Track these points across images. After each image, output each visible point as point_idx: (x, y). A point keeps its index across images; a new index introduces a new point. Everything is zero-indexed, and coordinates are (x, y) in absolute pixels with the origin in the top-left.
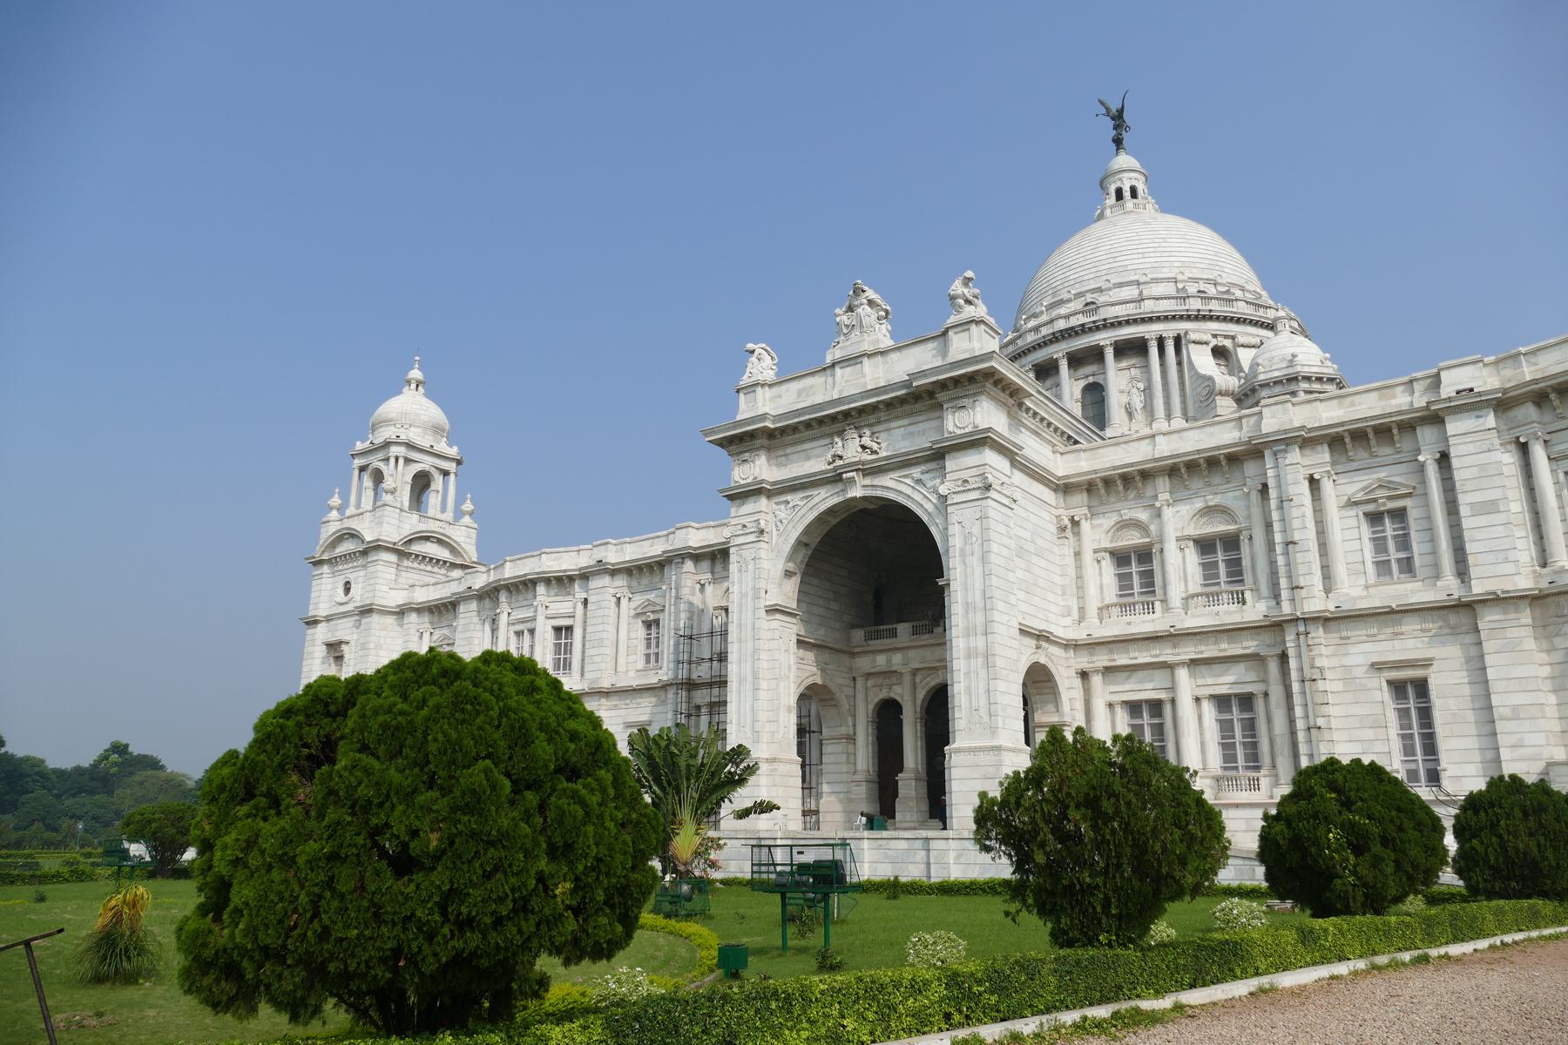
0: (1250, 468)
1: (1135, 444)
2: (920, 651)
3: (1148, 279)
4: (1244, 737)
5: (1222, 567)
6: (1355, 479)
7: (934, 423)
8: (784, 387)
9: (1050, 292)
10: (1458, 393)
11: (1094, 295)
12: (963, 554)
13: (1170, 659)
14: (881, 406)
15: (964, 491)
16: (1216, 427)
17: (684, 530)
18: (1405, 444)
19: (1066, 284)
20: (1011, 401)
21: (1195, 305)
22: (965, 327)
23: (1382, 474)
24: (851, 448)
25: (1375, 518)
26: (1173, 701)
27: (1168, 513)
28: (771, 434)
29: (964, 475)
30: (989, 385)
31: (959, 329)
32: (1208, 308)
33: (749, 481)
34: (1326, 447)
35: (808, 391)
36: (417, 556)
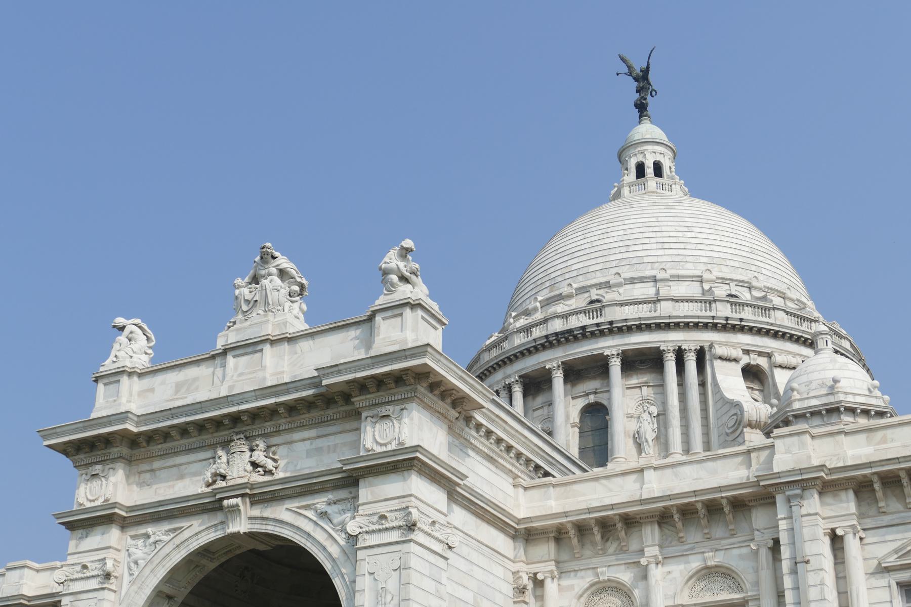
0: (759, 518)
1: (619, 480)
3: (667, 276)
6: (888, 538)
7: (349, 437)
8: (160, 378)
9: (548, 284)
11: (601, 292)
14: (281, 410)
15: (380, 530)
16: (720, 463)
17: (18, 572)
19: (567, 276)
20: (454, 413)
21: (723, 311)
22: (397, 311)
29: (382, 508)
30: (422, 389)
31: (389, 313)
32: (738, 316)
34: (851, 494)
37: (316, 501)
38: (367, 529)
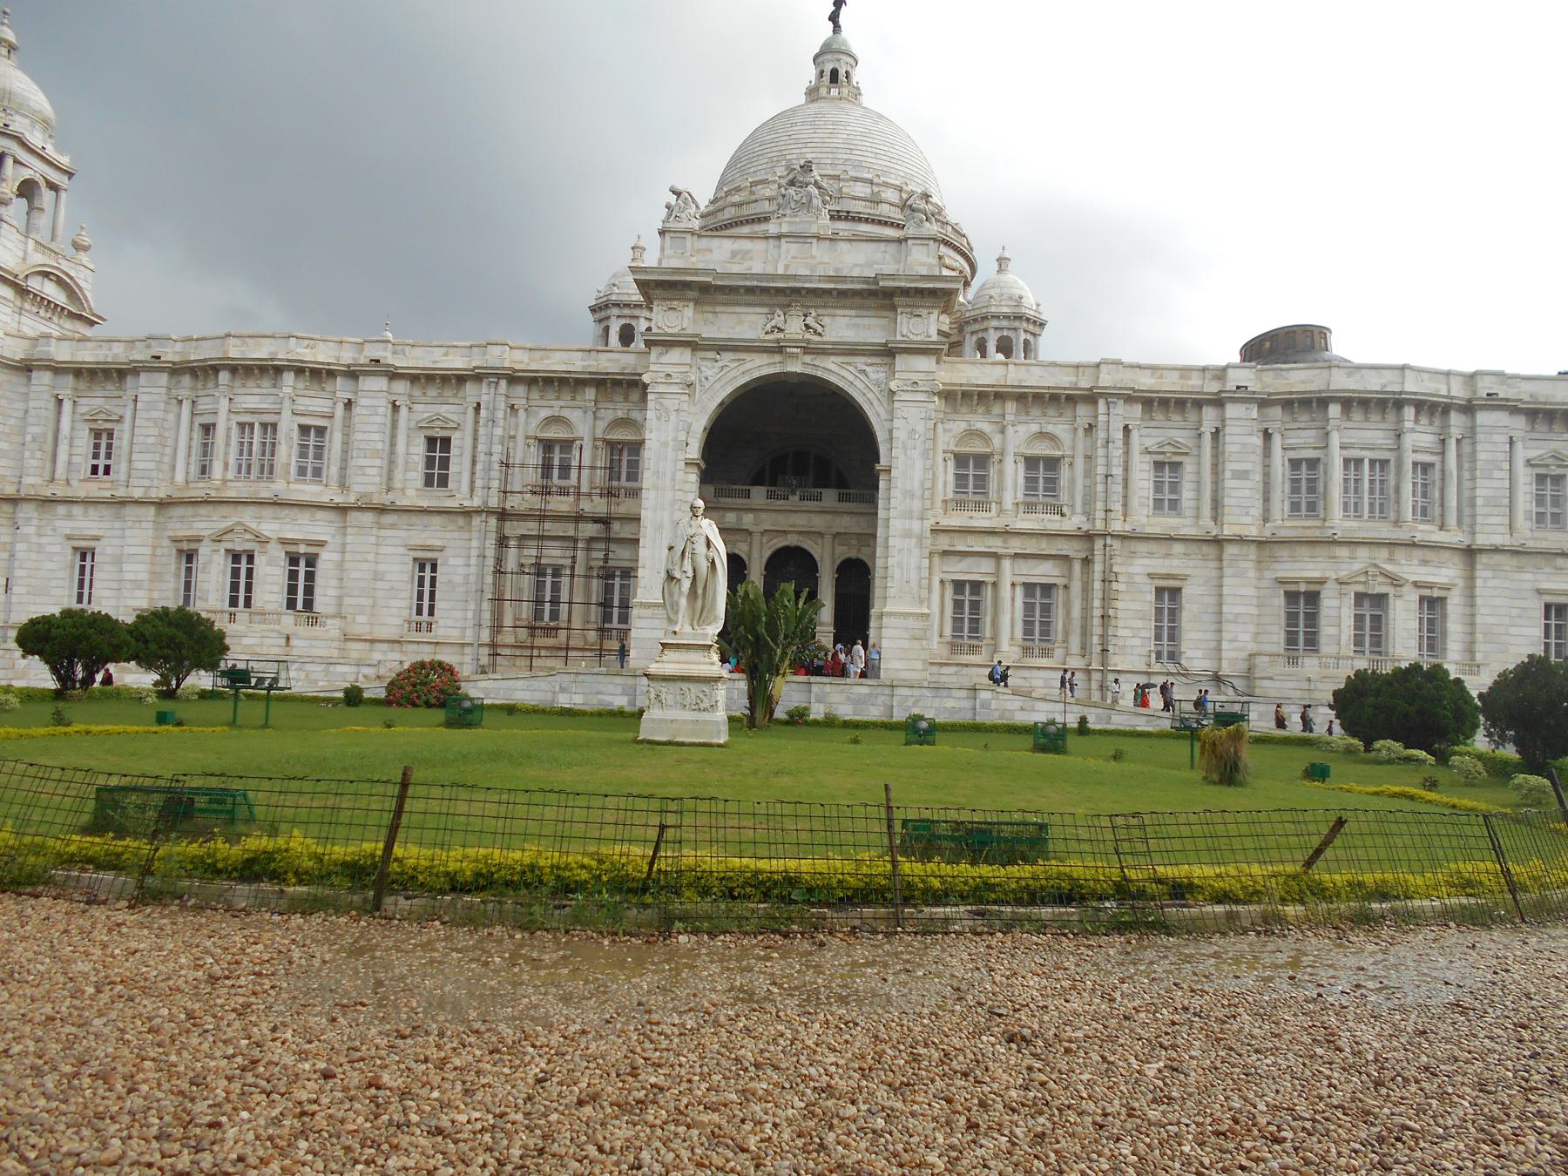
0: (1083, 410)
2: (774, 515)
5: (1041, 480)
9: (784, 163)
10: (1238, 388)
13: (1000, 551)
16: (1057, 369)
18: (1192, 416)
24: (794, 327)
25: (1159, 466)
26: (995, 584)
27: (1010, 430)
28: (705, 289)
29: (915, 377)
31: (919, 242)
33: (675, 331)
35: (745, 255)
36: (35, 295)
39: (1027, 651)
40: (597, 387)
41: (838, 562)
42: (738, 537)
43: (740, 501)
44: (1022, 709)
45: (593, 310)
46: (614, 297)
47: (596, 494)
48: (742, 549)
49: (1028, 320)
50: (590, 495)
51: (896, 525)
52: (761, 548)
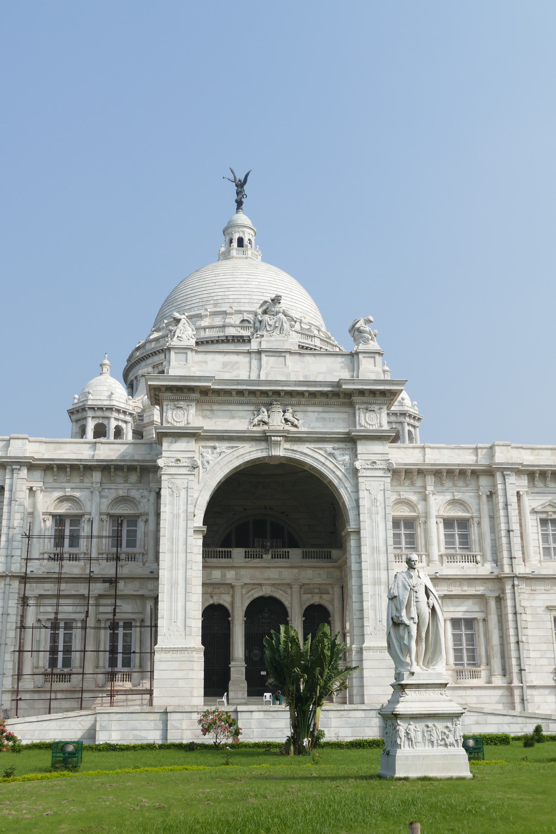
0: (484, 481)
1: (411, 450)
2: (251, 571)
4: (467, 645)
5: (457, 537)
6: (536, 498)
9: (212, 302)
12: (370, 513)
16: (462, 451)
17: (21, 441)
23: (549, 498)
25: (544, 522)
28: (205, 392)
29: (374, 458)
31: (367, 355)
33: (182, 425)
34: (526, 477)
37: (325, 446)
38: (365, 467)
39: (459, 673)
40: (102, 471)
41: (305, 607)
42: (222, 590)
43: (224, 560)
44: (477, 723)
45: (71, 413)
46: (90, 402)
47: (102, 559)
48: (225, 600)
49: (410, 416)
50: (97, 559)
51: (367, 575)
52: (242, 597)
